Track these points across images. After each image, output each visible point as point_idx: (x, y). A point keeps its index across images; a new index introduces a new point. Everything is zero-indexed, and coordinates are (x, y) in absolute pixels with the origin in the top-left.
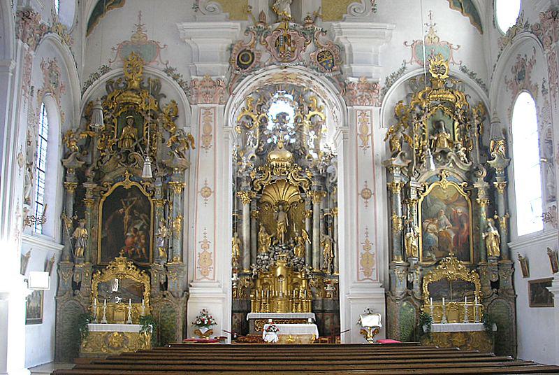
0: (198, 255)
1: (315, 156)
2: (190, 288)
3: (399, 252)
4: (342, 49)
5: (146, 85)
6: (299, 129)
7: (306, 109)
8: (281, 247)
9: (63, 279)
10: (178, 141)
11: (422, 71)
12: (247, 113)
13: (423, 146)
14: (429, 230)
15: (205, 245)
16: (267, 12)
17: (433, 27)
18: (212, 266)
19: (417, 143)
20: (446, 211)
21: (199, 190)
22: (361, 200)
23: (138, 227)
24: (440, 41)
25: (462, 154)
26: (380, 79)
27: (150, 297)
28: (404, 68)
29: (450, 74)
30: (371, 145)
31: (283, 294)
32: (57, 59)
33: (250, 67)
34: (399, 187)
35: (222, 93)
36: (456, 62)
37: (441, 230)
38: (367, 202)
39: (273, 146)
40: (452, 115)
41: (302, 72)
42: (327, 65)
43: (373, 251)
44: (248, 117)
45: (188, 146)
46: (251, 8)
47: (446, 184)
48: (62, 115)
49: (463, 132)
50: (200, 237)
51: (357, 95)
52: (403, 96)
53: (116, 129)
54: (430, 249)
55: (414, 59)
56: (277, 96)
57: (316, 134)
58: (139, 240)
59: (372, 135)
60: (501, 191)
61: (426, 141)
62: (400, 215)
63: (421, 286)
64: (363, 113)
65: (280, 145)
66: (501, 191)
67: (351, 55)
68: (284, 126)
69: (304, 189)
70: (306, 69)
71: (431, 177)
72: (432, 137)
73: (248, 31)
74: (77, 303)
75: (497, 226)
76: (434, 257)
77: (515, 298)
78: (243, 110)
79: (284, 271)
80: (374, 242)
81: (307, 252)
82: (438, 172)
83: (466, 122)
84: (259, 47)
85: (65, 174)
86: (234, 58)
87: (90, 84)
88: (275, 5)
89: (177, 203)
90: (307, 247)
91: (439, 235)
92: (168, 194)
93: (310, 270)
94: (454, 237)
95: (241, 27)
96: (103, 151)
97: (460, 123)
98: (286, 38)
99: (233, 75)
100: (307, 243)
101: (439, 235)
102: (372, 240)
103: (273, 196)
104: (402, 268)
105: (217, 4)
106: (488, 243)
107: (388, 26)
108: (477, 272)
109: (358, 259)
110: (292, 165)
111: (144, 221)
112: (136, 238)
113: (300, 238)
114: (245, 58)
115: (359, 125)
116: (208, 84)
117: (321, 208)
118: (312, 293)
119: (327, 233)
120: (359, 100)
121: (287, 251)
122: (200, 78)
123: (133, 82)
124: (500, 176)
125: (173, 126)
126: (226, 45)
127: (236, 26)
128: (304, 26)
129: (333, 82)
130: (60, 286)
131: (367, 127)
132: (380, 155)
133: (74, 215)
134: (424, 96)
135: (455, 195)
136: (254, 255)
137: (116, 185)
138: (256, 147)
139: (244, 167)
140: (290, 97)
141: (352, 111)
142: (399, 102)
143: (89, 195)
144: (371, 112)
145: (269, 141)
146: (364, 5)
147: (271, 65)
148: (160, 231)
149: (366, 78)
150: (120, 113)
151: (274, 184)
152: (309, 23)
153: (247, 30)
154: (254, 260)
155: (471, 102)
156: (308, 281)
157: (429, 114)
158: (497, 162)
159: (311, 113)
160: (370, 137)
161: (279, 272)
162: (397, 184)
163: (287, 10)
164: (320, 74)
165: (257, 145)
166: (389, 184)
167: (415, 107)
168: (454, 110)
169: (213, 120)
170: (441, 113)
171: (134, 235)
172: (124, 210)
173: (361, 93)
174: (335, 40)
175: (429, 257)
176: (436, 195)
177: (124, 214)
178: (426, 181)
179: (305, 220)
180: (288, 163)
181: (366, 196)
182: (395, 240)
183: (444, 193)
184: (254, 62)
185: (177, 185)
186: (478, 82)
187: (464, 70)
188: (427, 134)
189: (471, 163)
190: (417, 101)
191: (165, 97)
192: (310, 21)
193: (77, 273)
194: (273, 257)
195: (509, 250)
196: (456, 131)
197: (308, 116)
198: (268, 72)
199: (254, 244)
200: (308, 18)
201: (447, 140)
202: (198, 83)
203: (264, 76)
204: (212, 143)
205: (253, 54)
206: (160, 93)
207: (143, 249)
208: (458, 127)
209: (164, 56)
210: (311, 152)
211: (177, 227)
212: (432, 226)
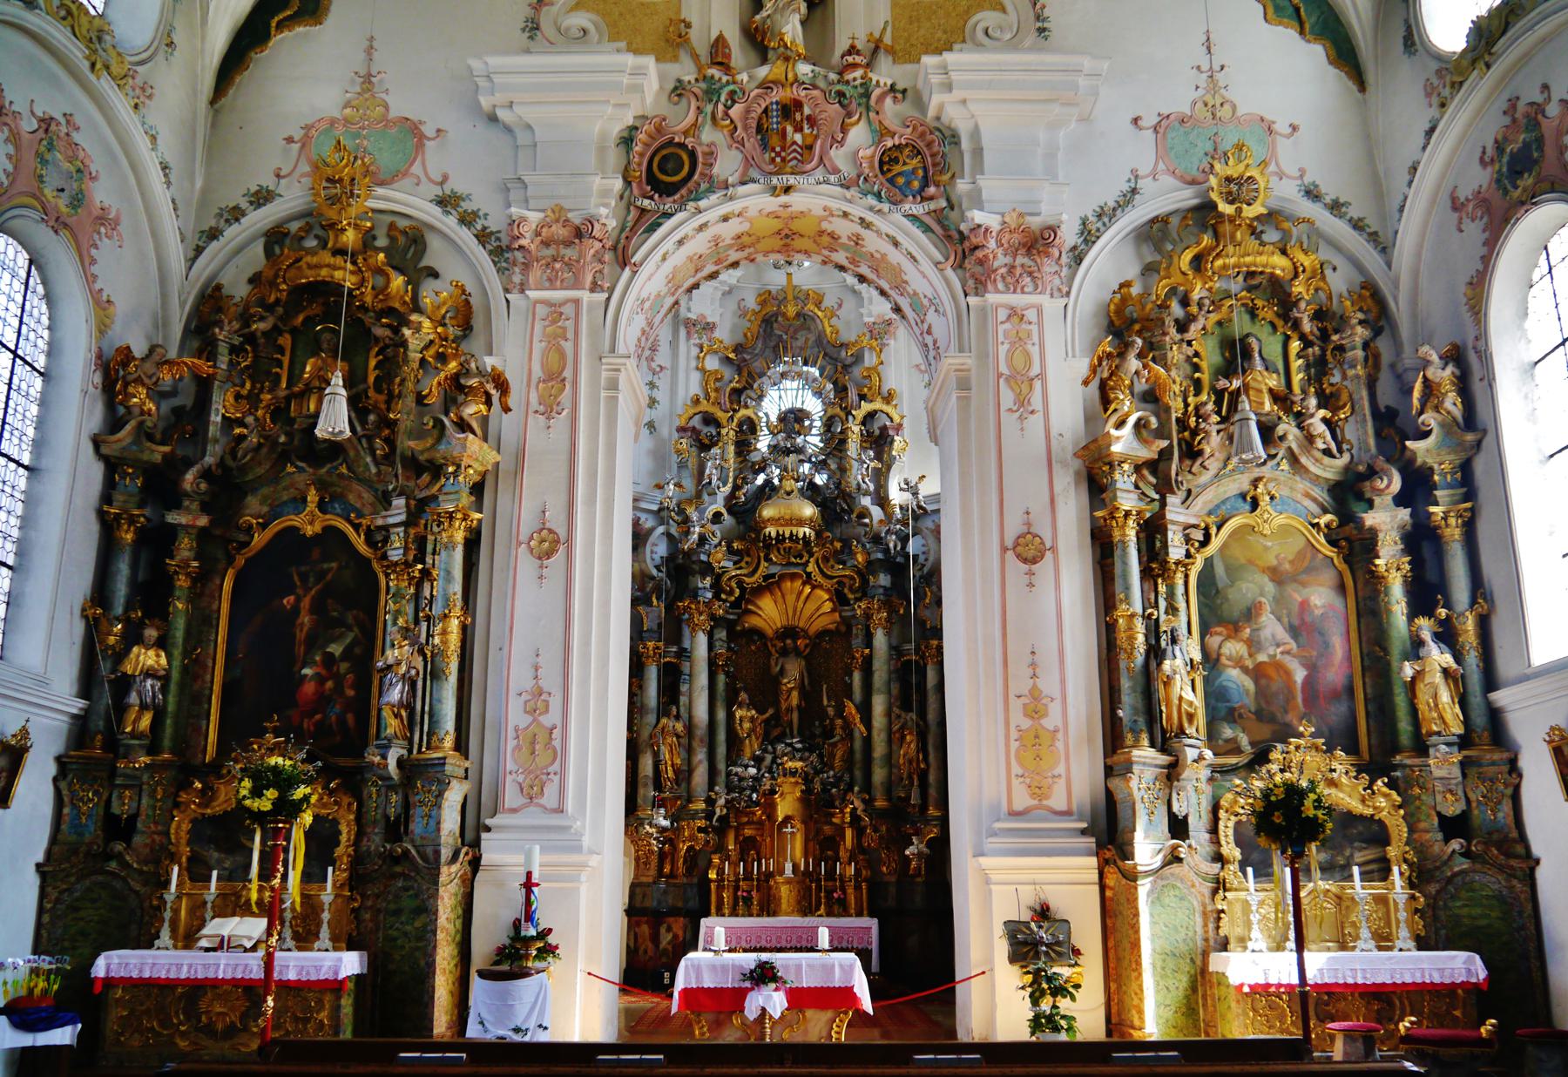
0: (511, 733)
1: (877, 513)
2: (484, 835)
3: (1141, 720)
4: (954, 138)
5: (382, 242)
6: (835, 444)
7: (853, 395)
8: (790, 745)
9: (74, 806)
10: (461, 388)
11: (1186, 198)
12: (705, 406)
13: (1197, 408)
14: (1224, 660)
15: (537, 701)
16: (734, 37)
17: (1218, 76)
18: (556, 766)
19: (1180, 400)
20: (1279, 601)
21: (522, 538)
22: (1016, 567)
23: (336, 649)
24: (1240, 112)
25: (1320, 429)
26: (1065, 217)
27: (357, 860)
28: (1134, 191)
29: (1274, 204)
30: (1040, 408)
31: (795, 867)
32: (78, 119)
33: (684, 191)
34: (1131, 523)
35: (601, 262)
36: (1287, 171)
37: (1262, 658)
38: (1031, 573)
39: (768, 491)
40: (1279, 323)
41: (836, 205)
42: (908, 183)
43: (1052, 720)
44: (709, 420)
45: (489, 403)
46: (688, 26)
47: (1272, 518)
48: (102, 305)
49: (1318, 370)
50: (520, 678)
51: (996, 264)
52: (1132, 271)
53: (286, 361)
54: (1233, 716)
55: (1161, 166)
56: (781, 368)
57: (878, 457)
58: (339, 689)
59: (1042, 376)
60: (1453, 532)
61: (1204, 397)
62: (1138, 608)
63: (1214, 830)
64: (1015, 314)
65: (789, 484)
66: (1453, 532)
67: (978, 152)
68: (800, 440)
69: (851, 596)
70: (848, 194)
71: (1223, 502)
72: (1222, 383)
73: (679, 90)
74: (118, 885)
75: (1447, 636)
76: (1244, 740)
77: (1532, 870)
78: (696, 401)
79: (797, 805)
80: (1057, 694)
81: (858, 756)
82: (1246, 486)
83: (1324, 336)
84: (708, 135)
85: (109, 485)
86: (640, 165)
87: (213, 234)
88: (758, 17)
89: (448, 572)
90: (858, 744)
91: (1257, 673)
92: (429, 548)
93: (864, 801)
94: (1308, 682)
95: (662, 77)
96: (240, 423)
97: (1307, 343)
98: (789, 110)
99: (633, 213)
100: (857, 734)
101: (1257, 673)
102: (1048, 684)
103: (769, 613)
104: (1149, 774)
105: (594, 17)
106: (1423, 697)
107: (1087, 63)
108: (1392, 785)
109: (1007, 745)
110: (818, 534)
111: (356, 629)
112: (329, 684)
113: (839, 722)
114: (670, 166)
115: (1003, 349)
116: (561, 232)
117: (894, 643)
118: (873, 864)
119: (906, 707)
120: (1003, 278)
121: (807, 754)
122: (534, 217)
123: (343, 230)
124: (1449, 486)
125: (456, 356)
126: (617, 129)
127: (640, 67)
128: (841, 73)
129: (927, 229)
130: (64, 827)
131: (1028, 355)
132: (1068, 436)
133: (129, 606)
134: (1198, 262)
135: (1300, 555)
136: (721, 766)
137: (276, 527)
138: (727, 489)
139: (696, 536)
140: (815, 371)
141: (983, 311)
142: (1122, 286)
143: (185, 548)
144: (1039, 311)
145: (760, 479)
146: (1012, 17)
147: (743, 183)
148: (391, 655)
149: (1021, 215)
150: (301, 318)
151: (770, 585)
152: (855, 66)
153: (676, 88)
154: (722, 779)
155: (1339, 282)
156: (859, 832)
157: (1214, 317)
158: (1440, 446)
159: (866, 407)
160: (1037, 384)
161: (785, 806)
162: (1127, 514)
163: (792, 29)
164: (886, 207)
165: (730, 485)
166: (1099, 514)
167: (1168, 296)
168: (1285, 304)
169: (570, 335)
170: (1246, 317)
171: (324, 672)
172: (298, 600)
173: (1008, 260)
174: (931, 113)
175: (1227, 741)
176: (1238, 553)
177: (296, 610)
178: (1210, 513)
179: (851, 676)
180: (807, 530)
181: (1030, 554)
182: (1125, 684)
183: (1266, 548)
184: (696, 177)
185: (451, 516)
186: (1357, 225)
187: (1312, 194)
188: (1205, 377)
189: (1346, 458)
190: (1176, 278)
191: (435, 274)
192: (858, 59)
193: (126, 787)
194: (770, 771)
195: (1495, 716)
196: (1296, 364)
197: (859, 414)
198: (735, 206)
199: (721, 736)
200: (852, 50)
201: (1271, 391)
202: (527, 230)
203: (725, 219)
204: (566, 397)
205: (692, 155)
206: (424, 263)
207: (350, 718)
208: (1299, 356)
209: (435, 160)
210: (866, 501)
211: (444, 642)
212: (1233, 648)
